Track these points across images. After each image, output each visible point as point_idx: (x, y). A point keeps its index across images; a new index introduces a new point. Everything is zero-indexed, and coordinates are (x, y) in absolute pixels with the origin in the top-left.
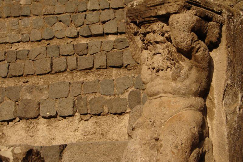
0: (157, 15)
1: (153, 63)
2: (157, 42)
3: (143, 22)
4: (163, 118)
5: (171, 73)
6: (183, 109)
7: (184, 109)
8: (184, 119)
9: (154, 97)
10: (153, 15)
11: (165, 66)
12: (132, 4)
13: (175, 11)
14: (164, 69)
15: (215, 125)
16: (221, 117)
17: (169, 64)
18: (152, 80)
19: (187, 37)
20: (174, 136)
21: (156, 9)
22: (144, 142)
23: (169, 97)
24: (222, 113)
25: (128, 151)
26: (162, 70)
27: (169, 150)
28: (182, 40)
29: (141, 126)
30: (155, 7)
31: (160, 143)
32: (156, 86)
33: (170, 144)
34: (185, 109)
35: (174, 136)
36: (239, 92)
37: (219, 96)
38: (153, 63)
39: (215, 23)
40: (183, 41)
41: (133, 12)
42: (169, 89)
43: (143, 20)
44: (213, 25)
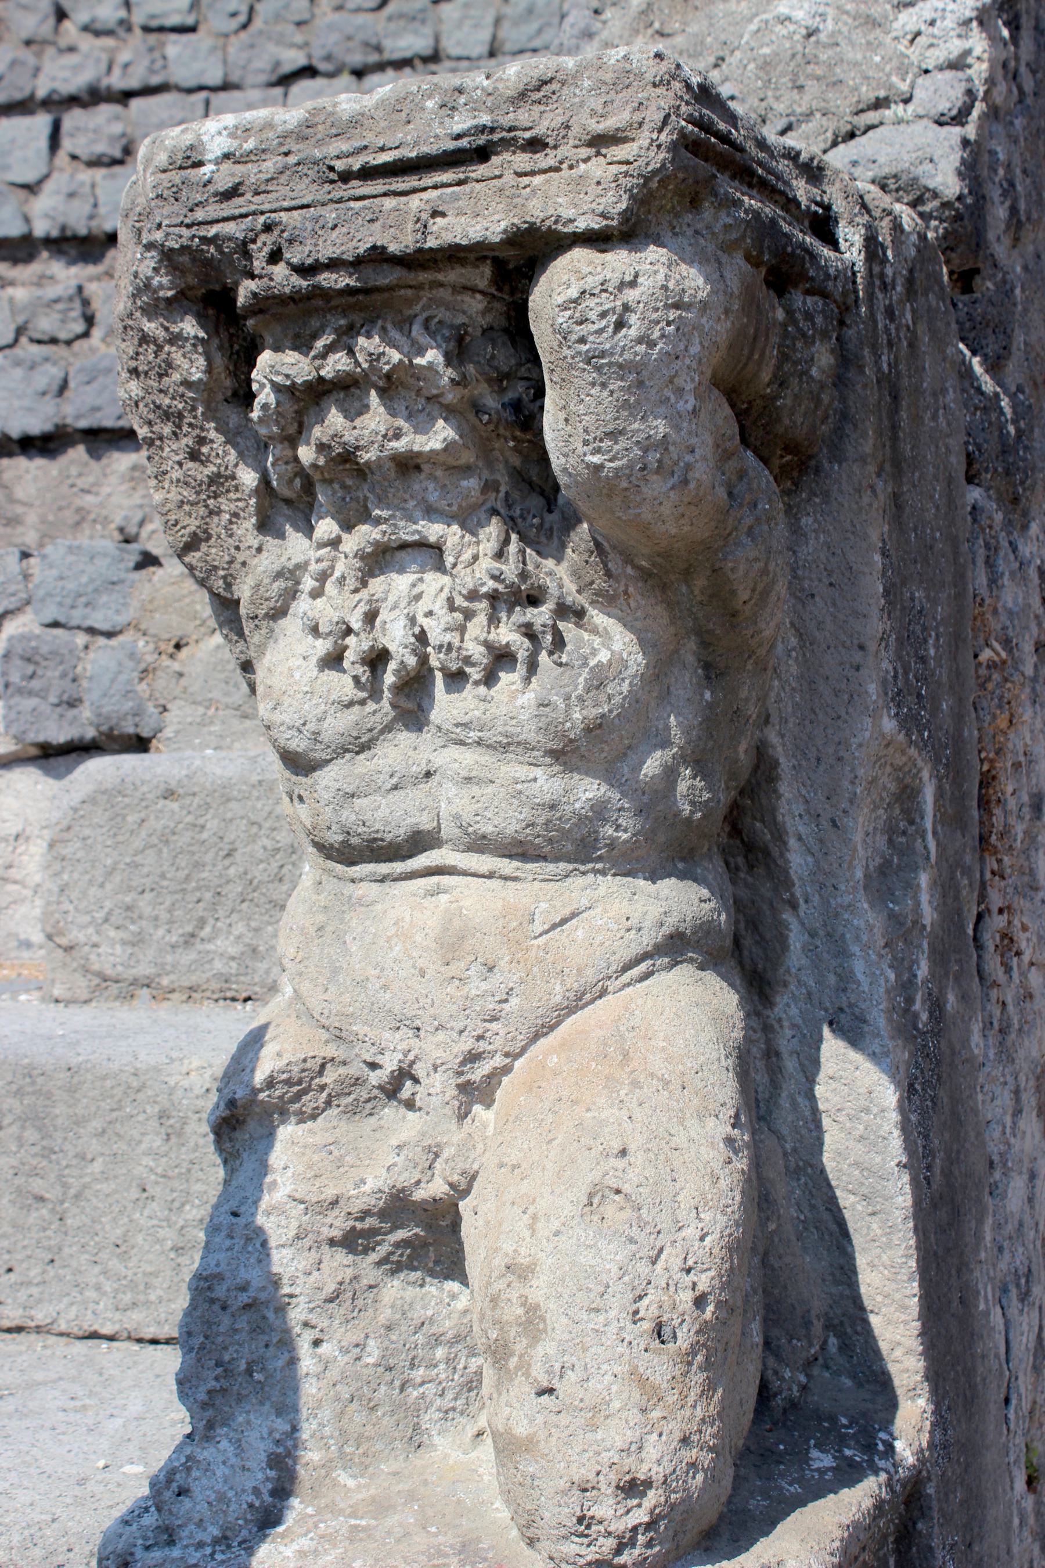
0: (431, 243)
1: (370, 617)
2: (408, 465)
3: (295, 298)
4: (482, 1046)
5: (529, 698)
6: (626, 968)
7: (636, 971)
8: (658, 1064)
9: (384, 868)
10: (393, 248)
11: (475, 650)
12: (192, 147)
13: (603, 215)
14: (468, 670)
15: (794, 1026)
16: (846, 979)
17: (506, 634)
18: (361, 745)
19: (690, 433)
20: (632, 1241)
21: (415, 191)
22: (337, 1224)
23: (506, 878)
24: (856, 949)
25: (212, 1301)
26: (456, 679)
27: (617, 1369)
28: (653, 457)
29: (297, 1097)
30: (411, 182)
31: (514, 1295)
32: (395, 788)
33: (612, 1314)
34: (643, 967)
35: (632, 1241)
36: (925, 774)
37: (825, 824)
38: (370, 617)
39: (816, 298)
40: (659, 461)
41: (200, 215)
42: (507, 820)
43: (299, 282)
44: (809, 316)
